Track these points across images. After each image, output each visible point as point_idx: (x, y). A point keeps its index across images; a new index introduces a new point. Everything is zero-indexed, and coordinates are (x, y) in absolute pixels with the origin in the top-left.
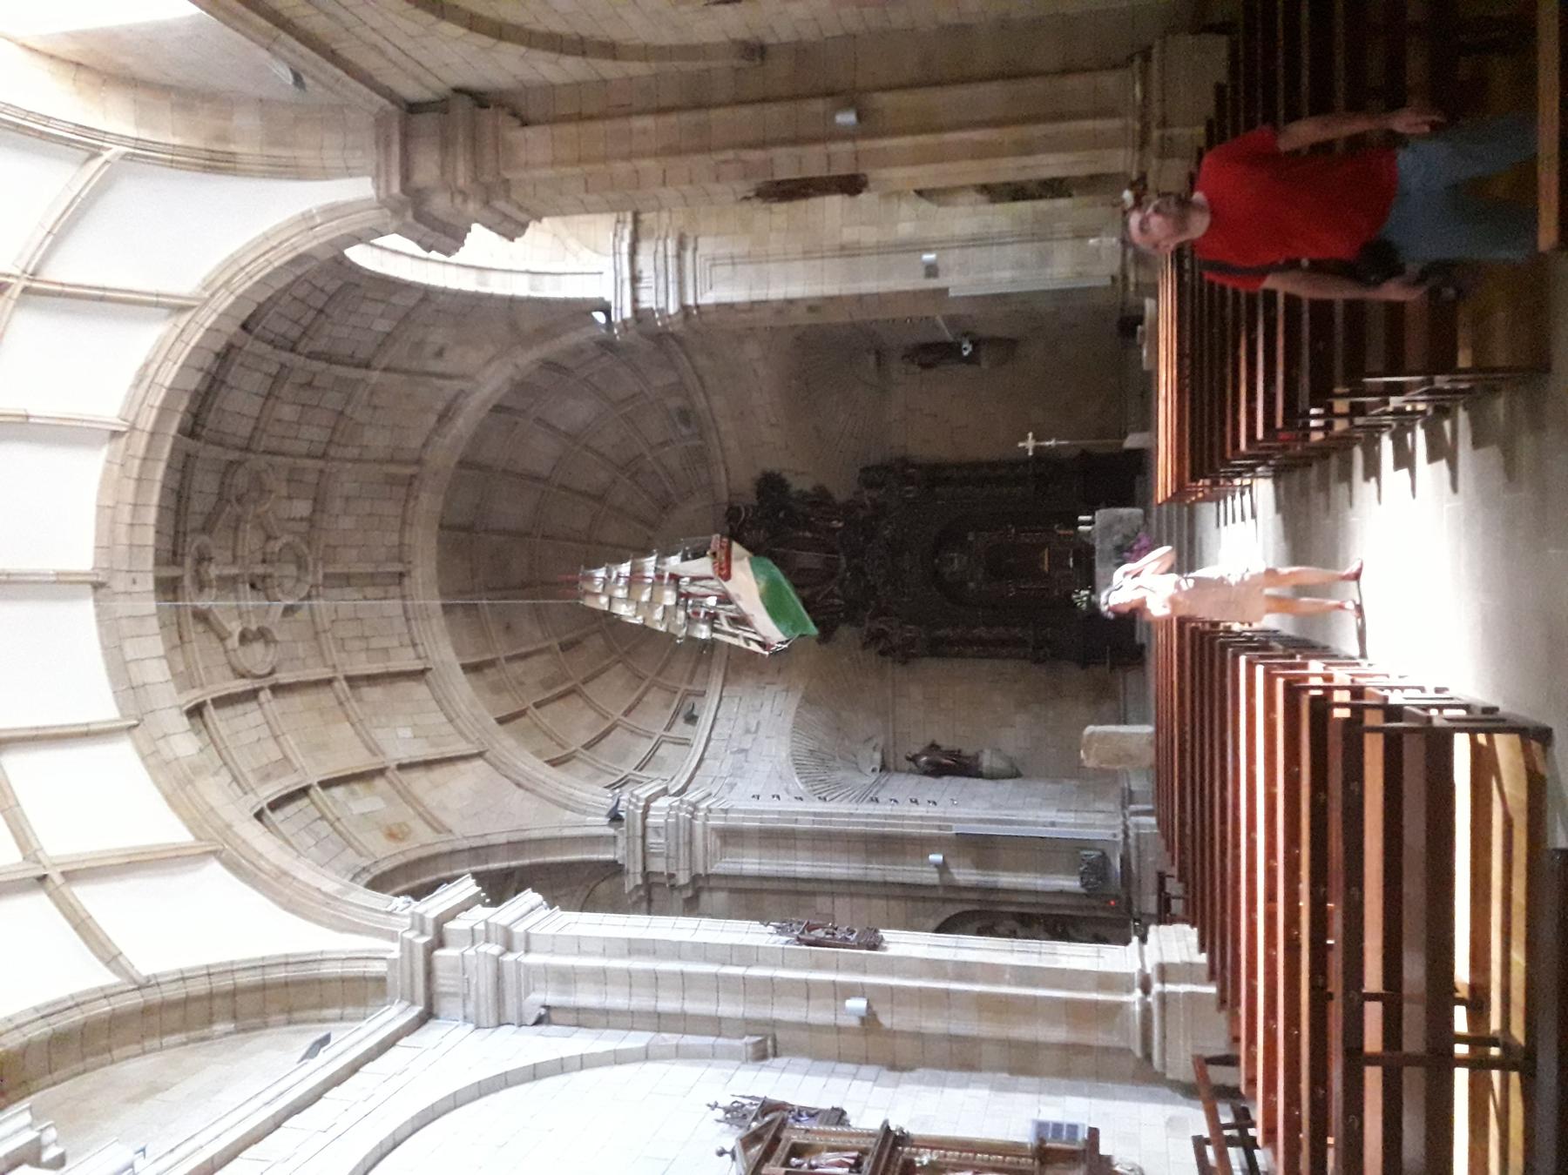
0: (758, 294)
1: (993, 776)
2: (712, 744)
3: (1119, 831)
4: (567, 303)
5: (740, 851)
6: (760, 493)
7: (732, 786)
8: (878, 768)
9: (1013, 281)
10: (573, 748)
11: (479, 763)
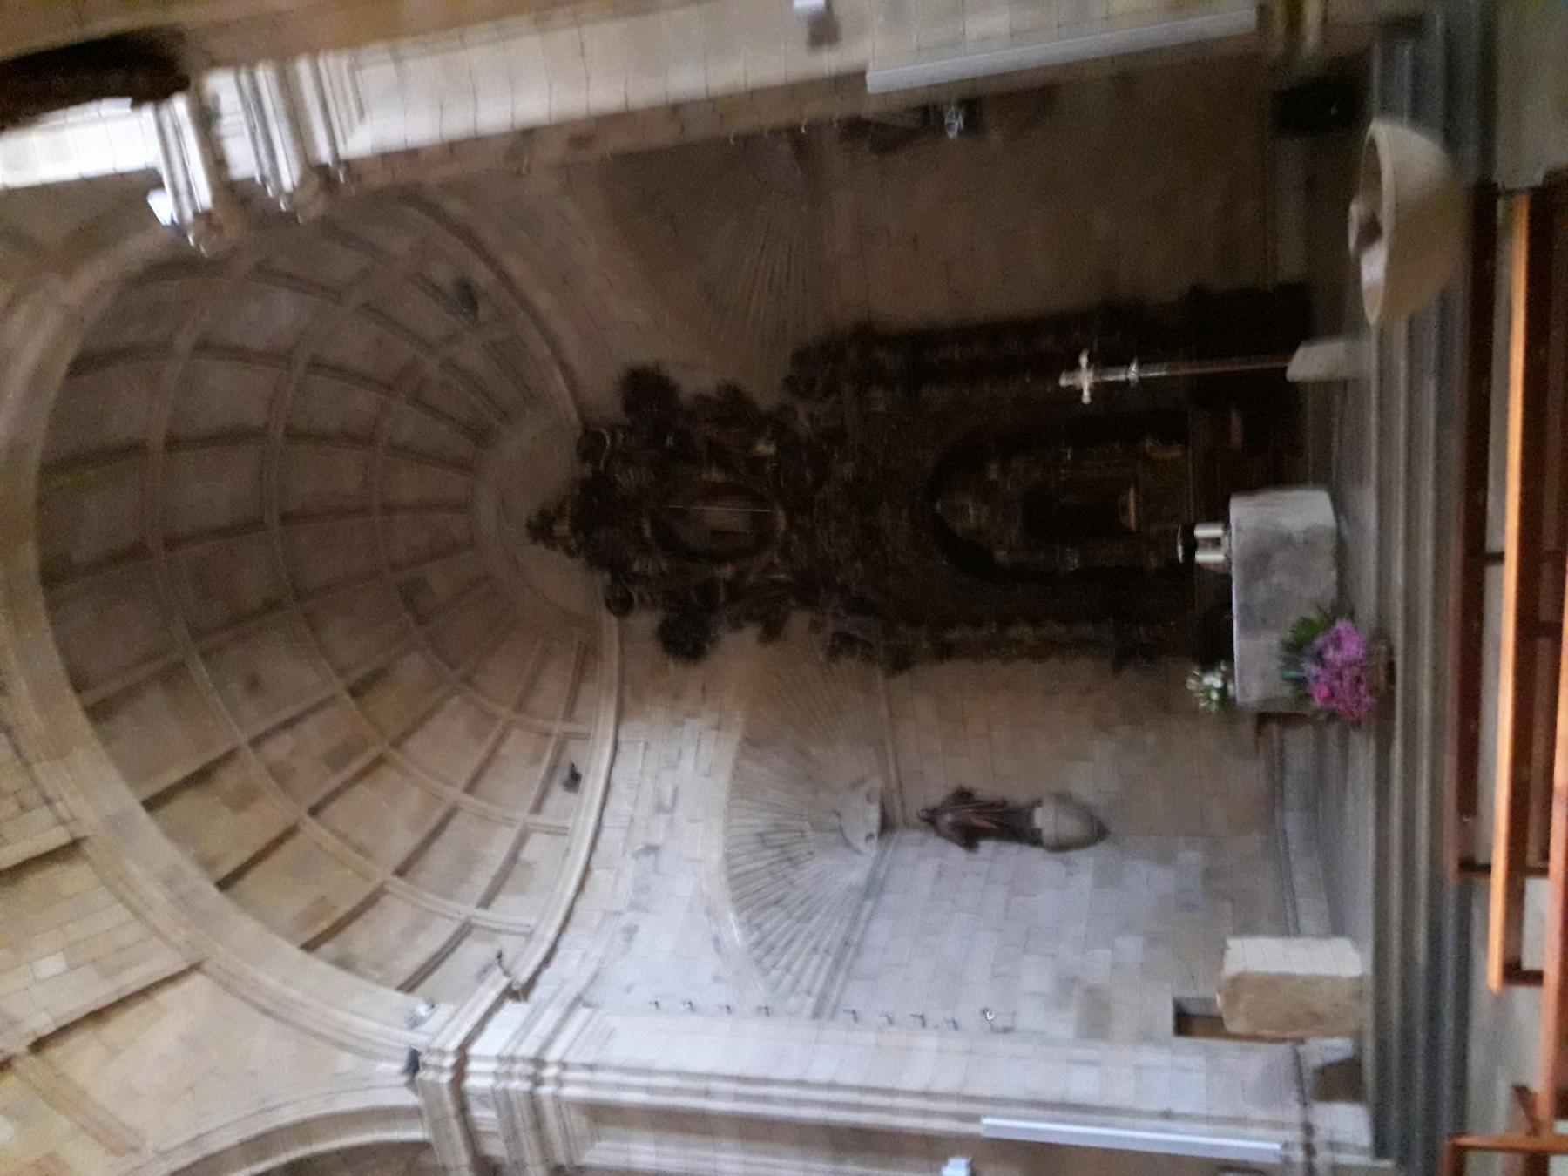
0: (457, 124)
1: (1061, 847)
2: (605, 835)
3: (1296, 1136)
4: (89, 186)
5: (622, 1132)
6: (629, 407)
7: (631, 932)
8: (875, 830)
9: (1015, 35)
10: (378, 880)
11: (197, 980)
